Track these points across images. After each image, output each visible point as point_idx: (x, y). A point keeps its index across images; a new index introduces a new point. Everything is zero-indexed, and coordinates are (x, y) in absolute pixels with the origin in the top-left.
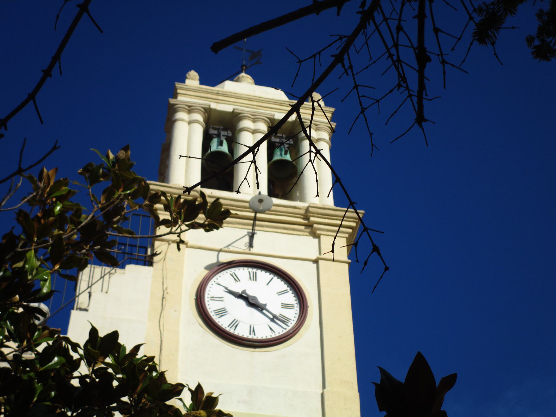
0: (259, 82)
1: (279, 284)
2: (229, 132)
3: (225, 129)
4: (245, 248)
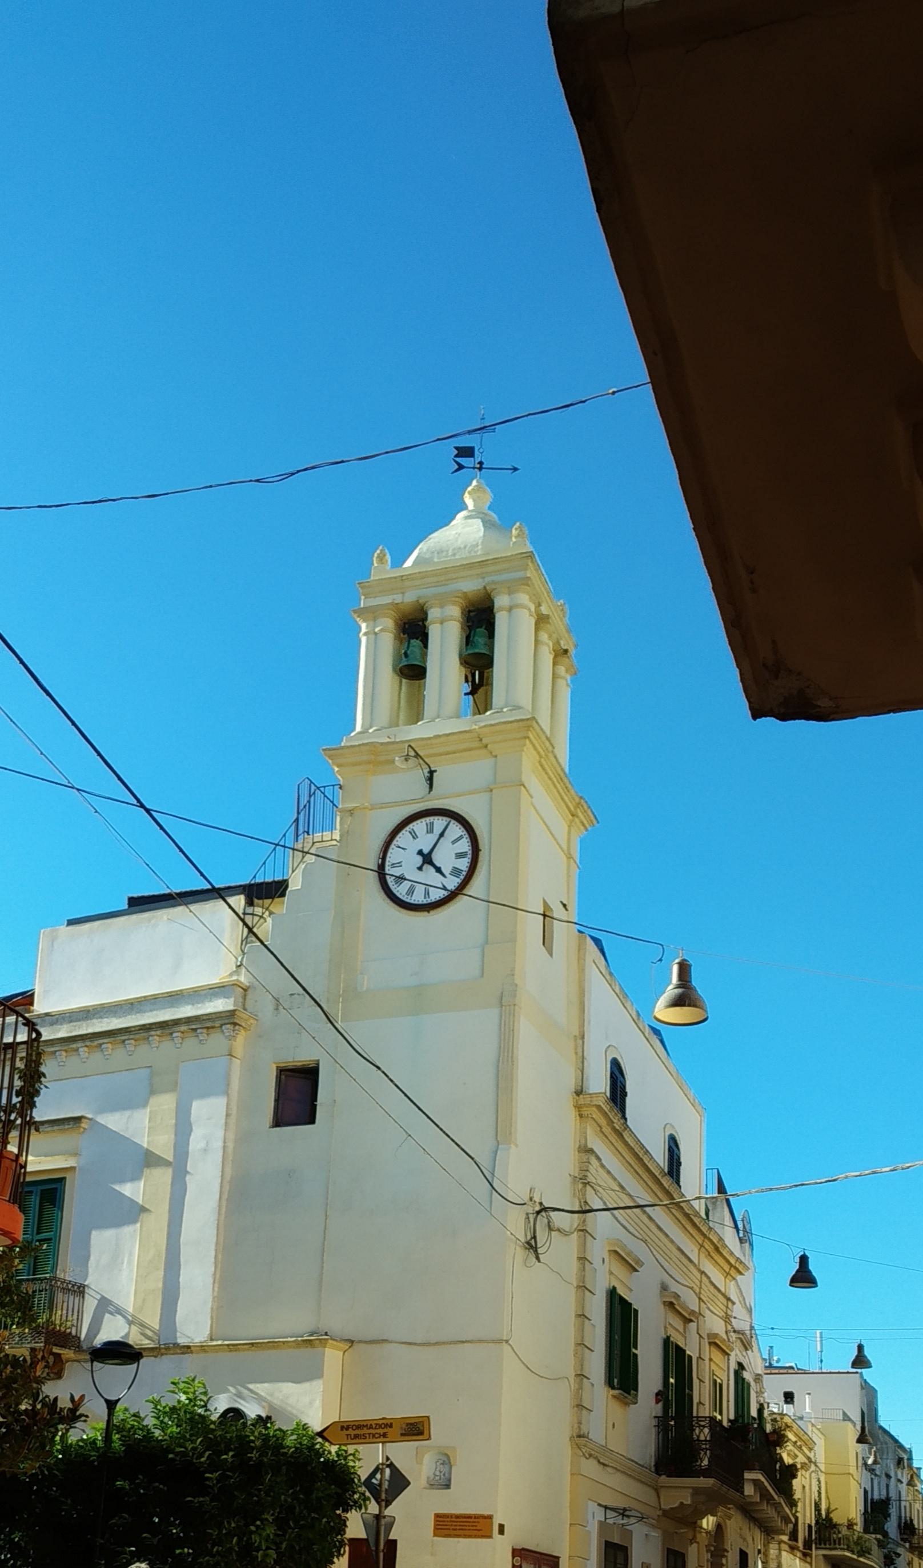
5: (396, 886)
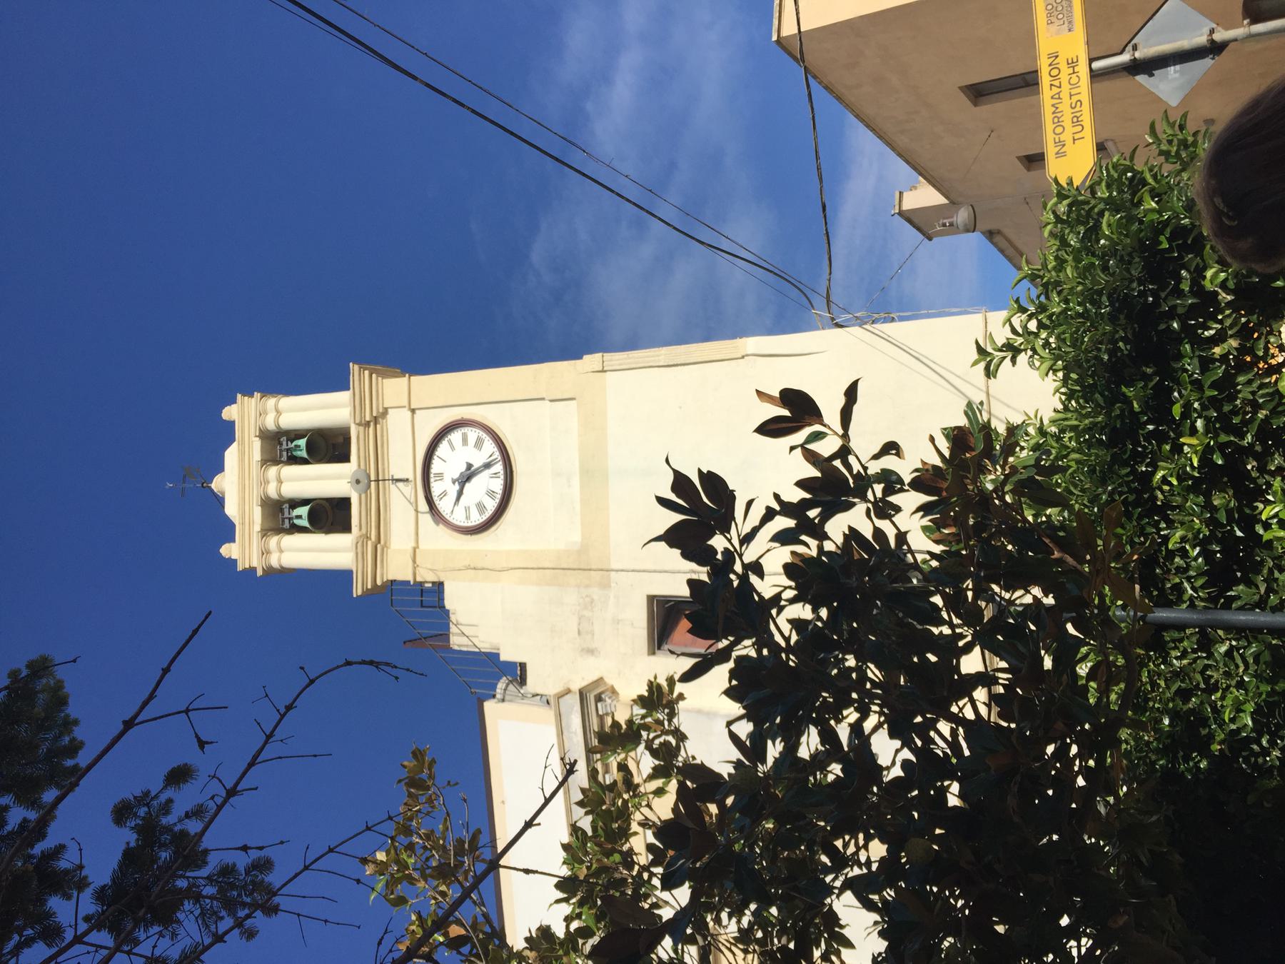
0: (220, 468)
1: (443, 449)
2: (284, 507)
3: (282, 511)
4: (410, 486)
5: (486, 513)
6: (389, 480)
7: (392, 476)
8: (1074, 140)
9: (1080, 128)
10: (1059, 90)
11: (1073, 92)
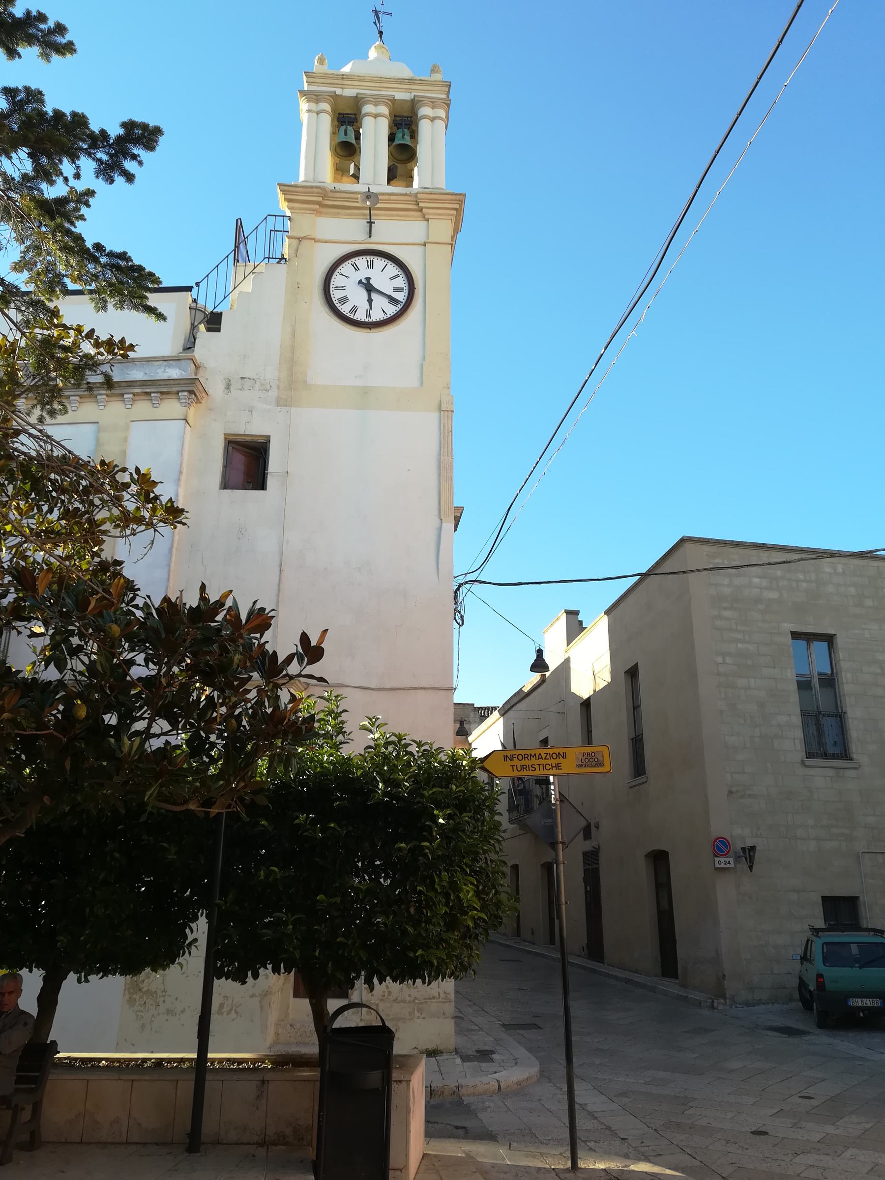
1: (392, 269)
6: (370, 219)
7: (374, 223)
8: (513, 766)
9: (519, 769)
10: (544, 758)
11: (541, 766)
